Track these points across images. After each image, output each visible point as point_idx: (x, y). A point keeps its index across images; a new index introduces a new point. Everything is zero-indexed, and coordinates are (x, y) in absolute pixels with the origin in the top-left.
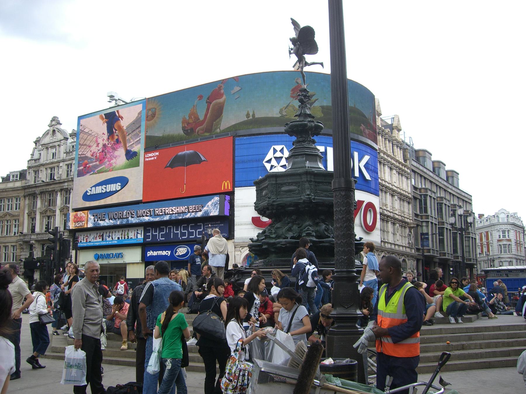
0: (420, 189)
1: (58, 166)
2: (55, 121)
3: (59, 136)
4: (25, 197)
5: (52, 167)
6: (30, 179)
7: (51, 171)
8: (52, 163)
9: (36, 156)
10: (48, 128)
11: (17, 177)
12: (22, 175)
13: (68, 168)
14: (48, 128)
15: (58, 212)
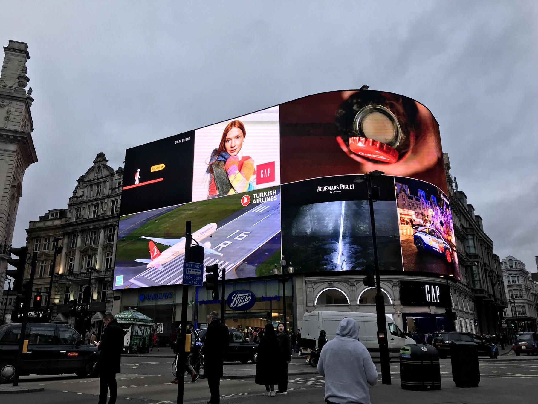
0: (466, 229)
1: (102, 203)
2: (101, 158)
3: (105, 172)
4: (64, 235)
5: (95, 203)
6: (72, 217)
7: (95, 208)
8: (96, 200)
9: (80, 193)
10: (93, 164)
11: (56, 215)
12: (62, 213)
13: (113, 204)
14: (93, 164)
15: (100, 250)
